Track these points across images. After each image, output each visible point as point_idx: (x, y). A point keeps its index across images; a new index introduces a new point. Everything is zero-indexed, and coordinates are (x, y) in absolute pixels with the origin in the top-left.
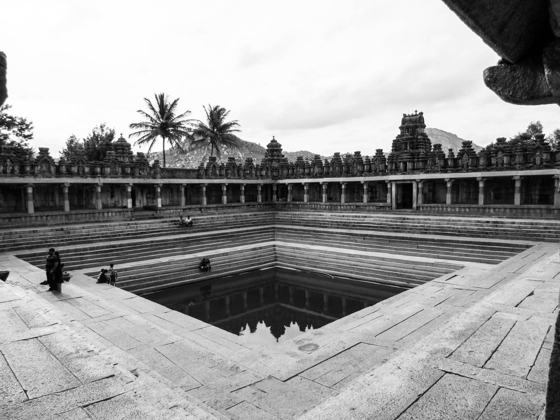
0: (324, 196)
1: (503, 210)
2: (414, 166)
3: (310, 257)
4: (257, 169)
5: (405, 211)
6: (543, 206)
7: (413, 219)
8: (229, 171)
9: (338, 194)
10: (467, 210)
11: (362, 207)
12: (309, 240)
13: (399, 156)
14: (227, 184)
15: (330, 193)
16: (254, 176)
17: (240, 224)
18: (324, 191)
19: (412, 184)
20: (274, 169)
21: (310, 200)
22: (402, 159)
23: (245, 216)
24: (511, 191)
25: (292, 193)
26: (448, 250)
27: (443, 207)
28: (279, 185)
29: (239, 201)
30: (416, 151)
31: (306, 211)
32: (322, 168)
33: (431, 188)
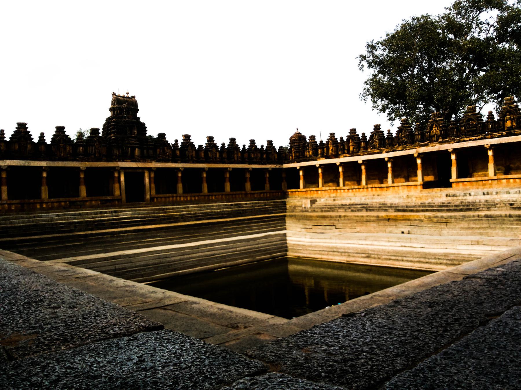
1: (220, 196)
3: (151, 262)
5: (140, 204)
6: (243, 192)
7: (173, 209)
10: (197, 198)
11: (78, 203)
22: (130, 144)
26: (246, 227)
27: (176, 197)
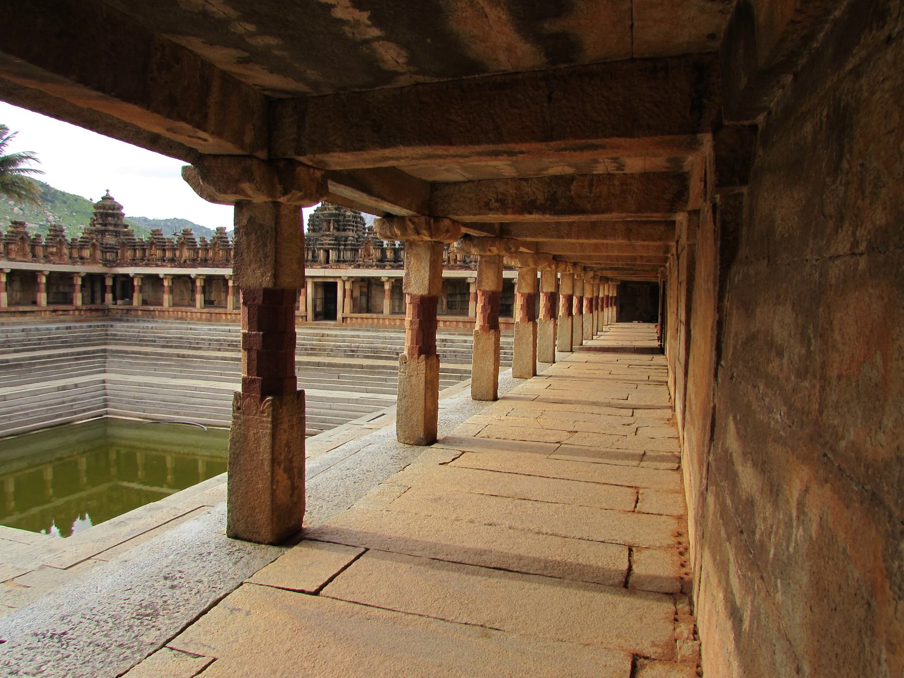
0: (199, 298)
2: (339, 257)
4: (72, 246)
7: (336, 336)
8: (12, 247)
9: (223, 295)
12: (169, 370)
13: (317, 240)
14: (8, 271)
15: (210, 293)
16: (66, 258)
17: (35, 344)
18: (199, 289)
19: (336, 283)
20: (106, 249)
21: (175, 305)
23: (48, 329)
24: (467, 299)
25: (141, 291)
26: (380, 379)
28: (116, 277)
29: (34, 303)
30: (344, 234)
31: (166, 323)
32: (196, 251)
33: (365, 290)
